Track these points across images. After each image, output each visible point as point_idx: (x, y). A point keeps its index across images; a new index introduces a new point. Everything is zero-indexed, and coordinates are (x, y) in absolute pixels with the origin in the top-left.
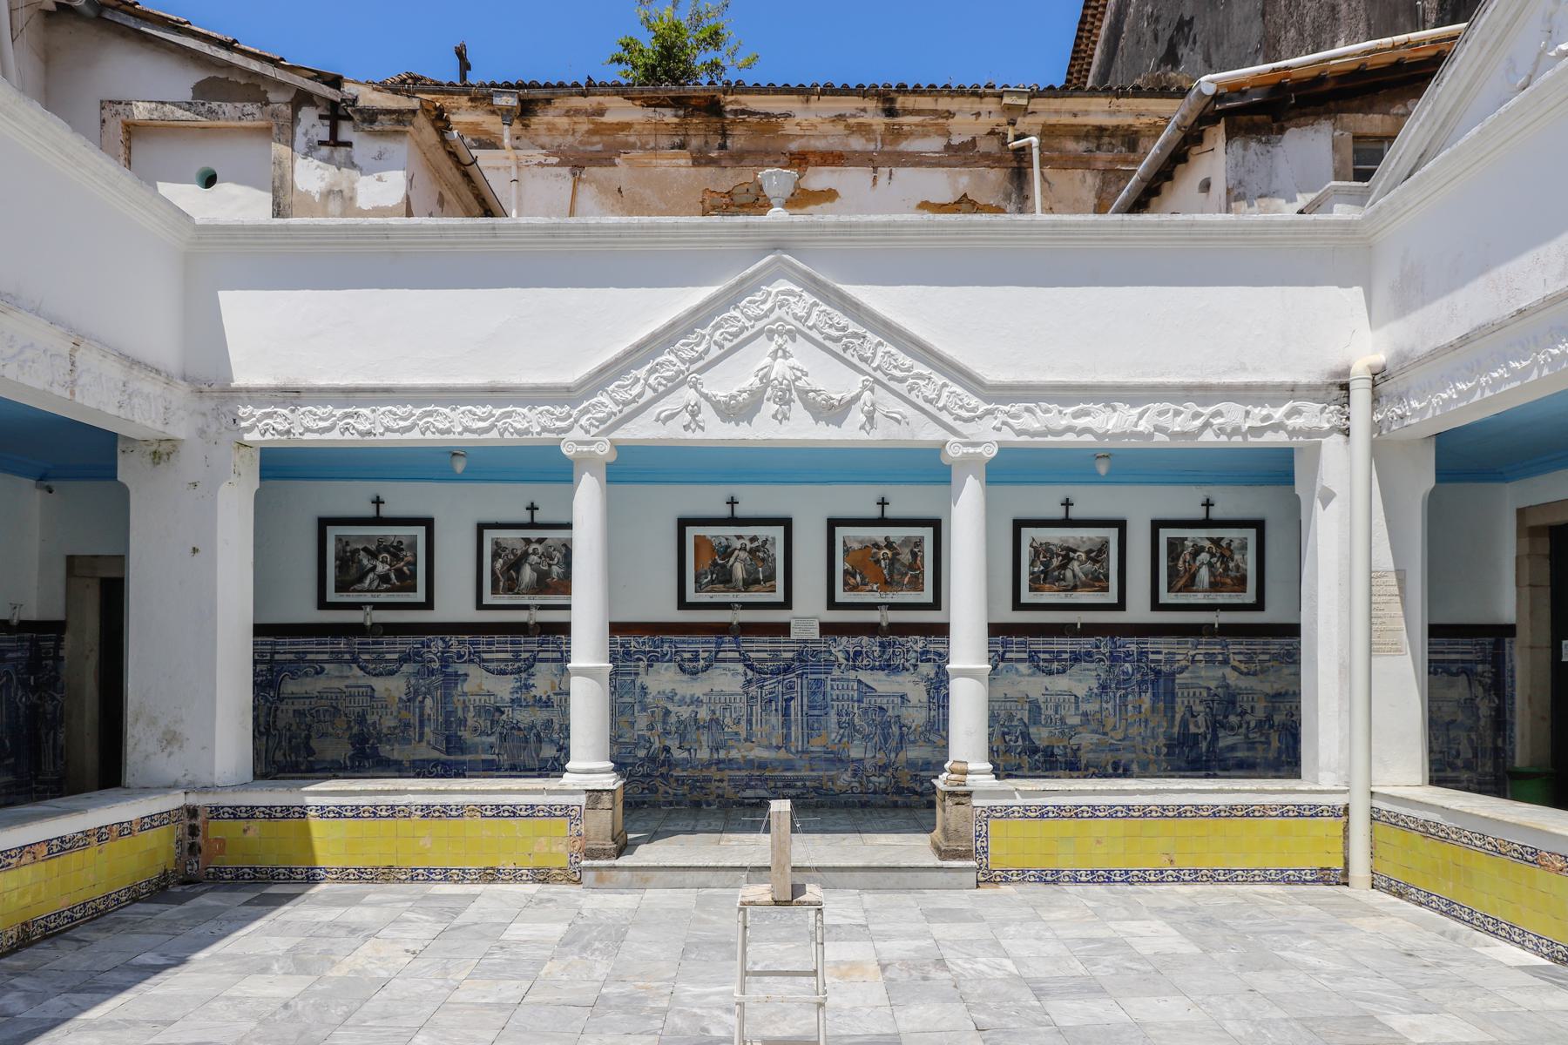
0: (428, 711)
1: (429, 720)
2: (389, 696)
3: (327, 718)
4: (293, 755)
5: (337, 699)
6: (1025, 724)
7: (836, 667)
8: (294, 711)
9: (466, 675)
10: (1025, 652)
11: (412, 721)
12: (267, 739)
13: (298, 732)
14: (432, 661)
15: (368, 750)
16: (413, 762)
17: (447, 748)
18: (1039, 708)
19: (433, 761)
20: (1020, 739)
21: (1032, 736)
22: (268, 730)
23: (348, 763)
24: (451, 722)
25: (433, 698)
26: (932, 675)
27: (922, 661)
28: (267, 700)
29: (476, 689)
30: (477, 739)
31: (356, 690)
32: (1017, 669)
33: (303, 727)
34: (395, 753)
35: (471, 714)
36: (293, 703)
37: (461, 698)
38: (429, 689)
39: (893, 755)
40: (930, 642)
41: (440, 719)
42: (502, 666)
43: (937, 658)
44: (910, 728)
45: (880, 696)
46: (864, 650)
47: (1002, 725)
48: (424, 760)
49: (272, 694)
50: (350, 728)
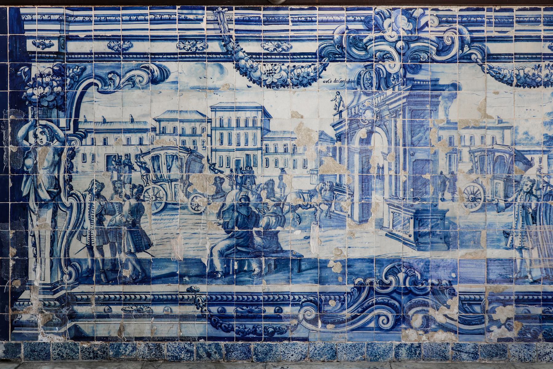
0: (377, 159)
1: (381, 177)
2: (299, 129)
3: (175, 173)
4: (107, 249)
5: (194, 134)
8: (108, 157)
9: (455, 86)
11: (345, 181)
12: (54, 214)
13: (117, 199)
14: (385, 57)
15: (258, 240)
16: (349, 264)
17: (417, 235)
19: (390, 261)
22: (55, 196)
23: (218, 266)
24: (425, 183)
25: (387, 132)
28: (53, 136)
29: (474, 116)
30: (478, 218)
31: (233, 115)
33: (127, 190)
34: (313, 243)
35: (466, 166)
36: (105, 143)
37: (445, 134)
38: (379, 114)
41: (403, 176)
42: (529, 68)
48: (371, 260)
49: (63, 122)
50: (220, 193)
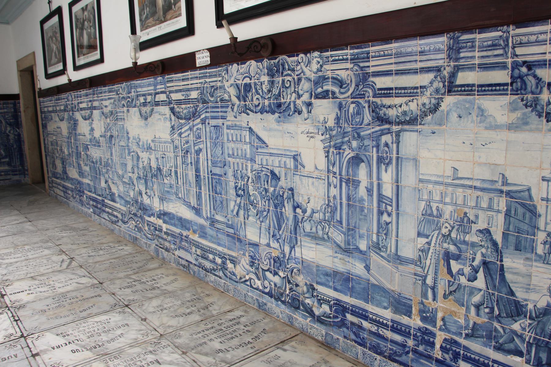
6: (495, 244)
7: (229, 109)
10: (503, 66)
18: (533, 211)
20: (481, 275)
21: (508, 276)
26: (331, 123)
27: (317, 97)
32: (482, 112)
39: (287, 249)
40: (327, 61)
43: (336, 90)
44: (304, 211)
45: (271, 154)
46: (253, 81)
47: (446, 237)
